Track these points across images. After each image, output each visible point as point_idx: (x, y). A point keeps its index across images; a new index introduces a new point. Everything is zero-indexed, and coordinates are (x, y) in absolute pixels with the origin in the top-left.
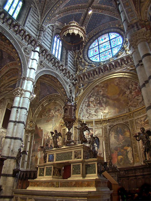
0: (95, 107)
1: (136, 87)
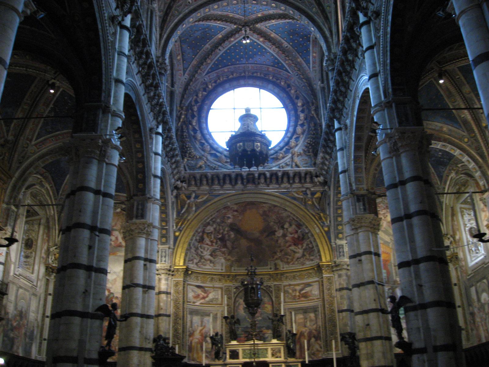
0: (212, 245)
1: (297, 229)
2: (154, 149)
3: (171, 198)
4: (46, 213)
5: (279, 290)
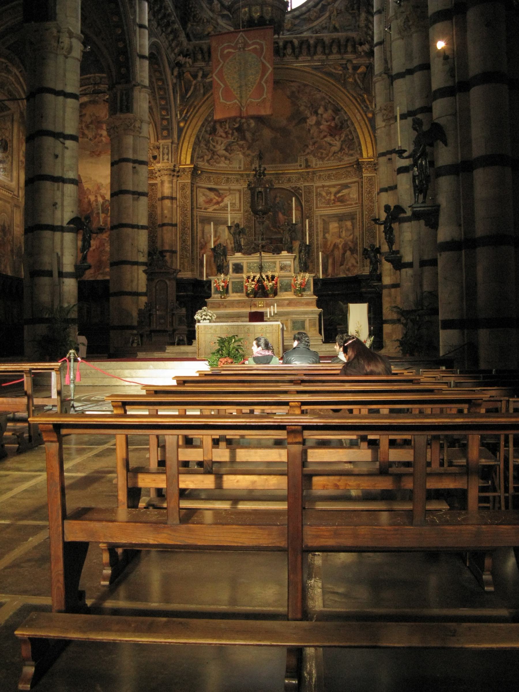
0: (227, 137)
1: (334, 115)
2: (137, 20)
3: (171, 80)
4: (19, 106)
5: (310, 193)
